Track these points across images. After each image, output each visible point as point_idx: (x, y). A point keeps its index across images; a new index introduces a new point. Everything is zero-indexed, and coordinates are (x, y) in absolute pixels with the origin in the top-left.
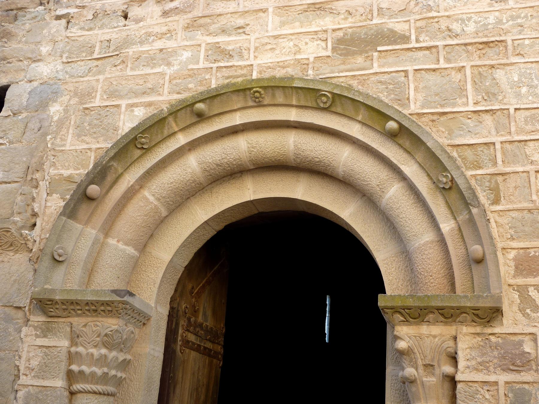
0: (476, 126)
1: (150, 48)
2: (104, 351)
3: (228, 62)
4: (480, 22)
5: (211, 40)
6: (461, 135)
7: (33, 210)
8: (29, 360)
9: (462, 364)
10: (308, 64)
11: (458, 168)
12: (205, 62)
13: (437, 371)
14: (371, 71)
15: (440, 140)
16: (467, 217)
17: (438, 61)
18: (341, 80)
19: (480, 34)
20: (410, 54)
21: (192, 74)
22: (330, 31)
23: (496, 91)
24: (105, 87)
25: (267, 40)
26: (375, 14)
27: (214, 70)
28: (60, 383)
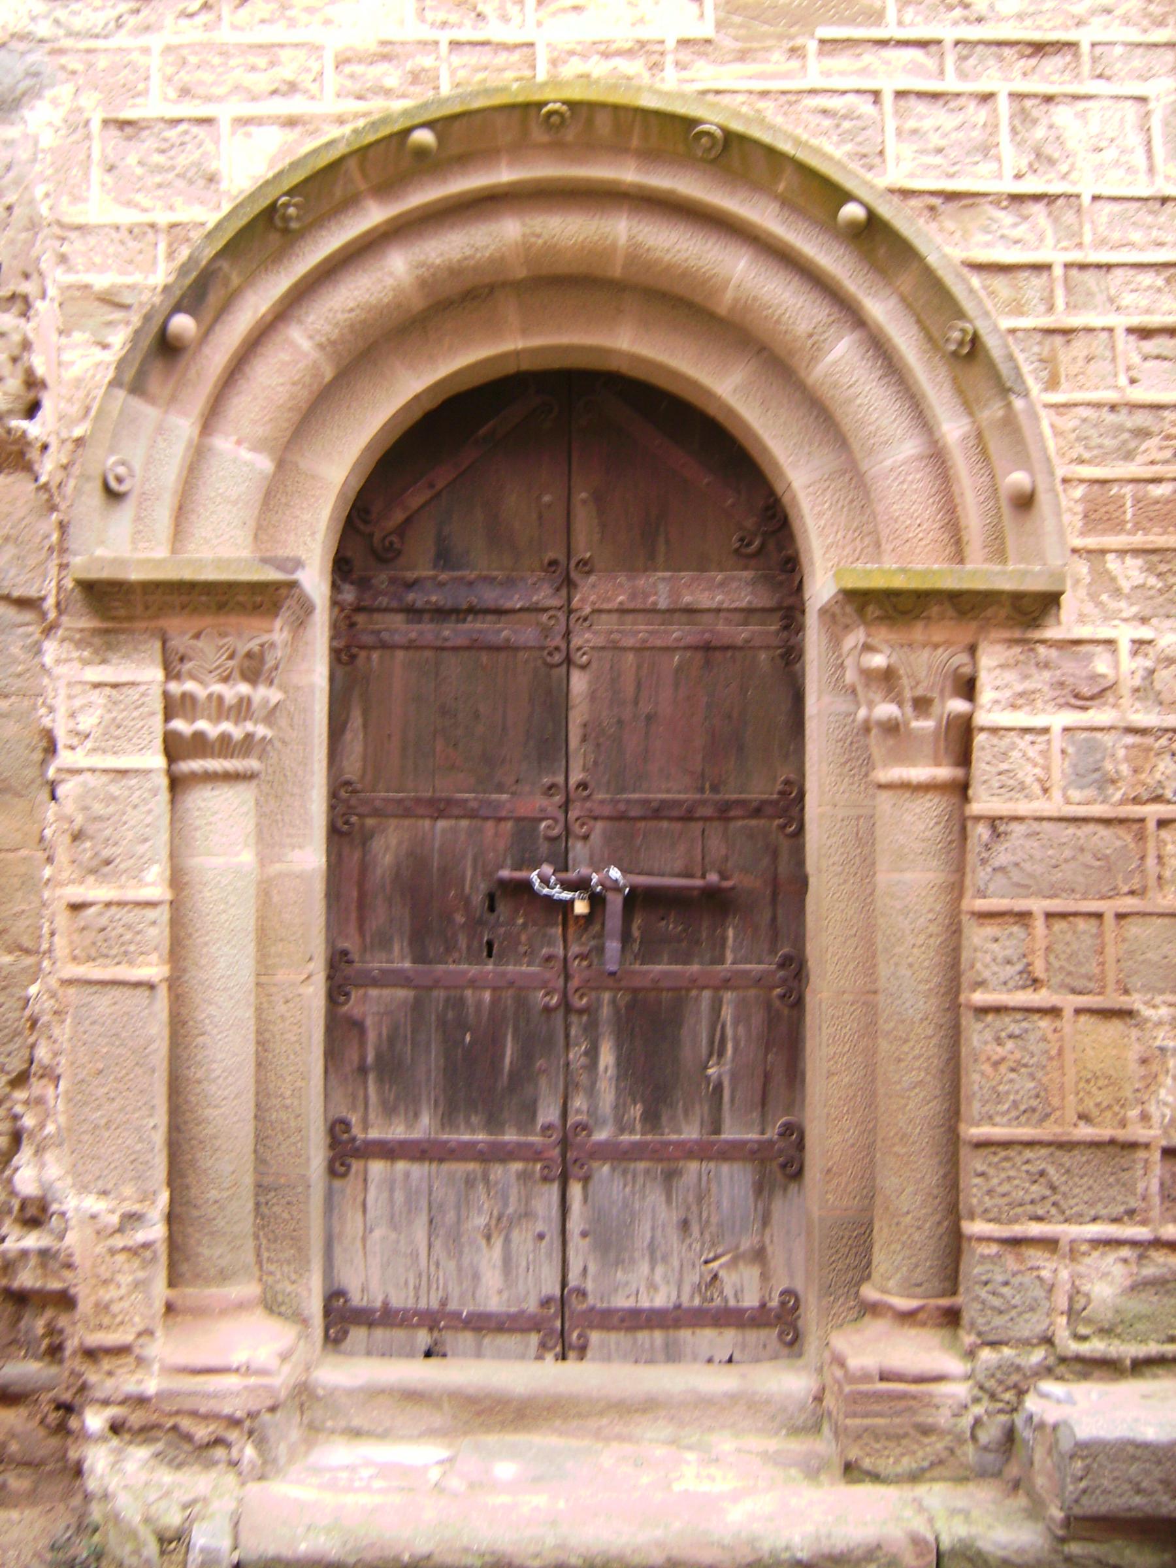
2: (244, 688)
6: (988, 245)
7: (30, 373)
8: (73, 715)
9: (986, 695)
11: (987, 314)
13: (936, 709)
15: (948, 250)
16: (1001, 413)
17: (942, 72)
18: (740, 98)
20: (889, 53)
21: (386, 53)
23: (1056, 155)
24: (170, 70)
27: (444, 48)
28: (157, 761)
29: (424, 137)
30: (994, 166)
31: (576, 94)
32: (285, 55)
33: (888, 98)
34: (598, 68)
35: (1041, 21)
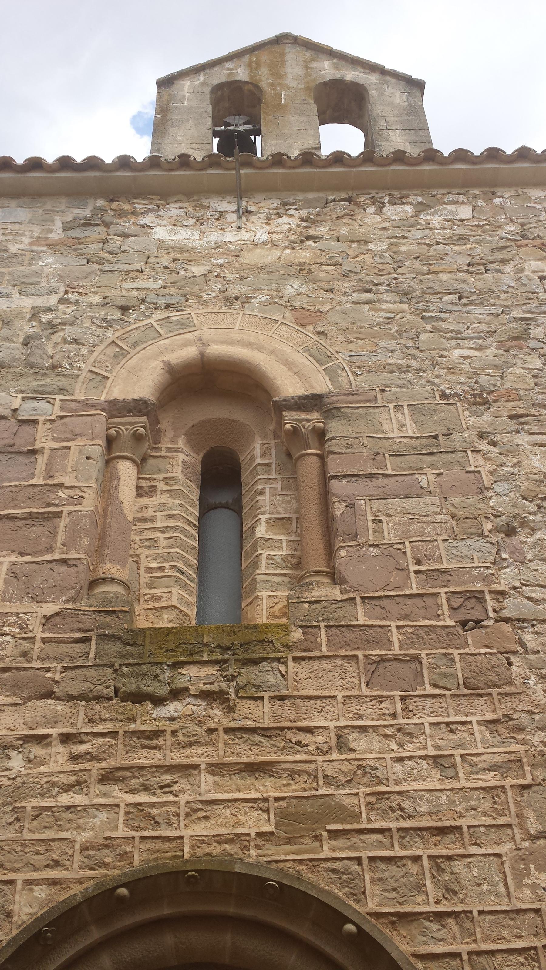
0: (439, 930)
1: (53, 804)
3: (153, 830)
4: (433, 801)
5: (131, 798)
6: (425, 943)
10: (248, 841)
12: (125, 829)
14: (322, 856)
18: (289, 865)
19: (434, 817)
21: (108, 843)
22: (271, 799)
23: (456, 889)
25: (200, 806)
26: (321, 782)
27: (137, 840)
29: (123, 891)
30: (424, 897)
31: (202, 867)
32: (54, 845)
33: (365, 862)
34: (216, 849)
35: (440, 815)
